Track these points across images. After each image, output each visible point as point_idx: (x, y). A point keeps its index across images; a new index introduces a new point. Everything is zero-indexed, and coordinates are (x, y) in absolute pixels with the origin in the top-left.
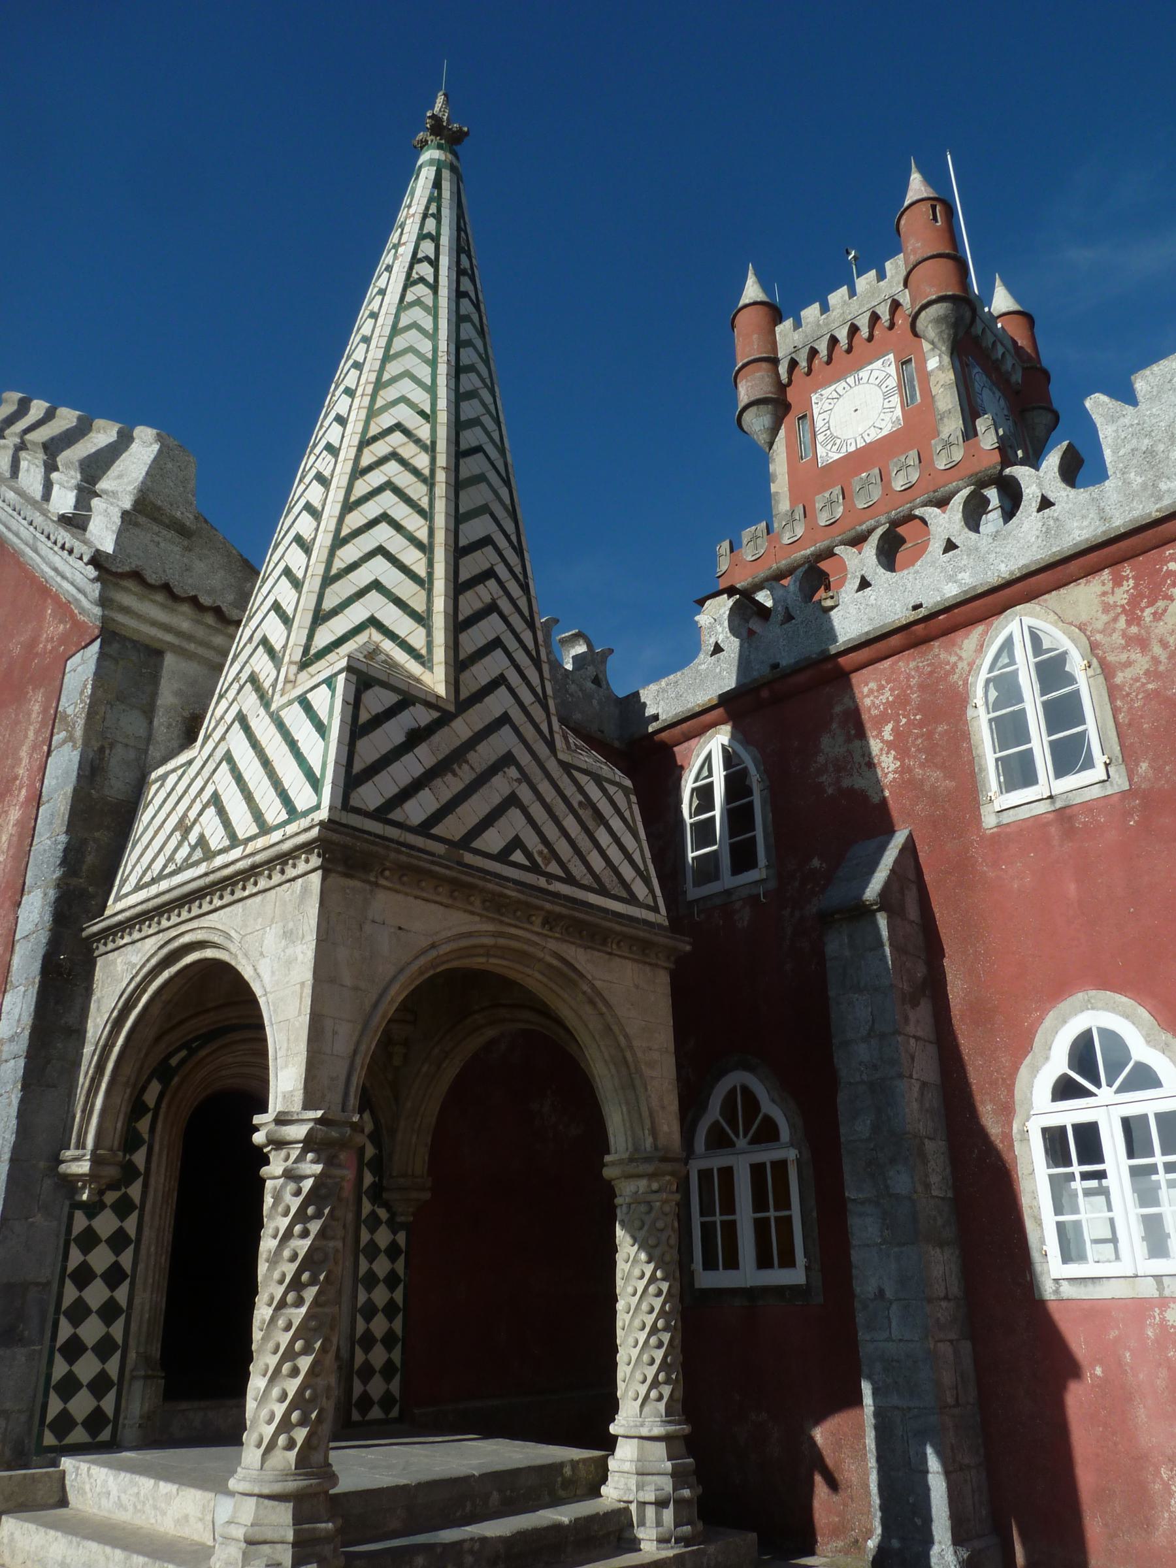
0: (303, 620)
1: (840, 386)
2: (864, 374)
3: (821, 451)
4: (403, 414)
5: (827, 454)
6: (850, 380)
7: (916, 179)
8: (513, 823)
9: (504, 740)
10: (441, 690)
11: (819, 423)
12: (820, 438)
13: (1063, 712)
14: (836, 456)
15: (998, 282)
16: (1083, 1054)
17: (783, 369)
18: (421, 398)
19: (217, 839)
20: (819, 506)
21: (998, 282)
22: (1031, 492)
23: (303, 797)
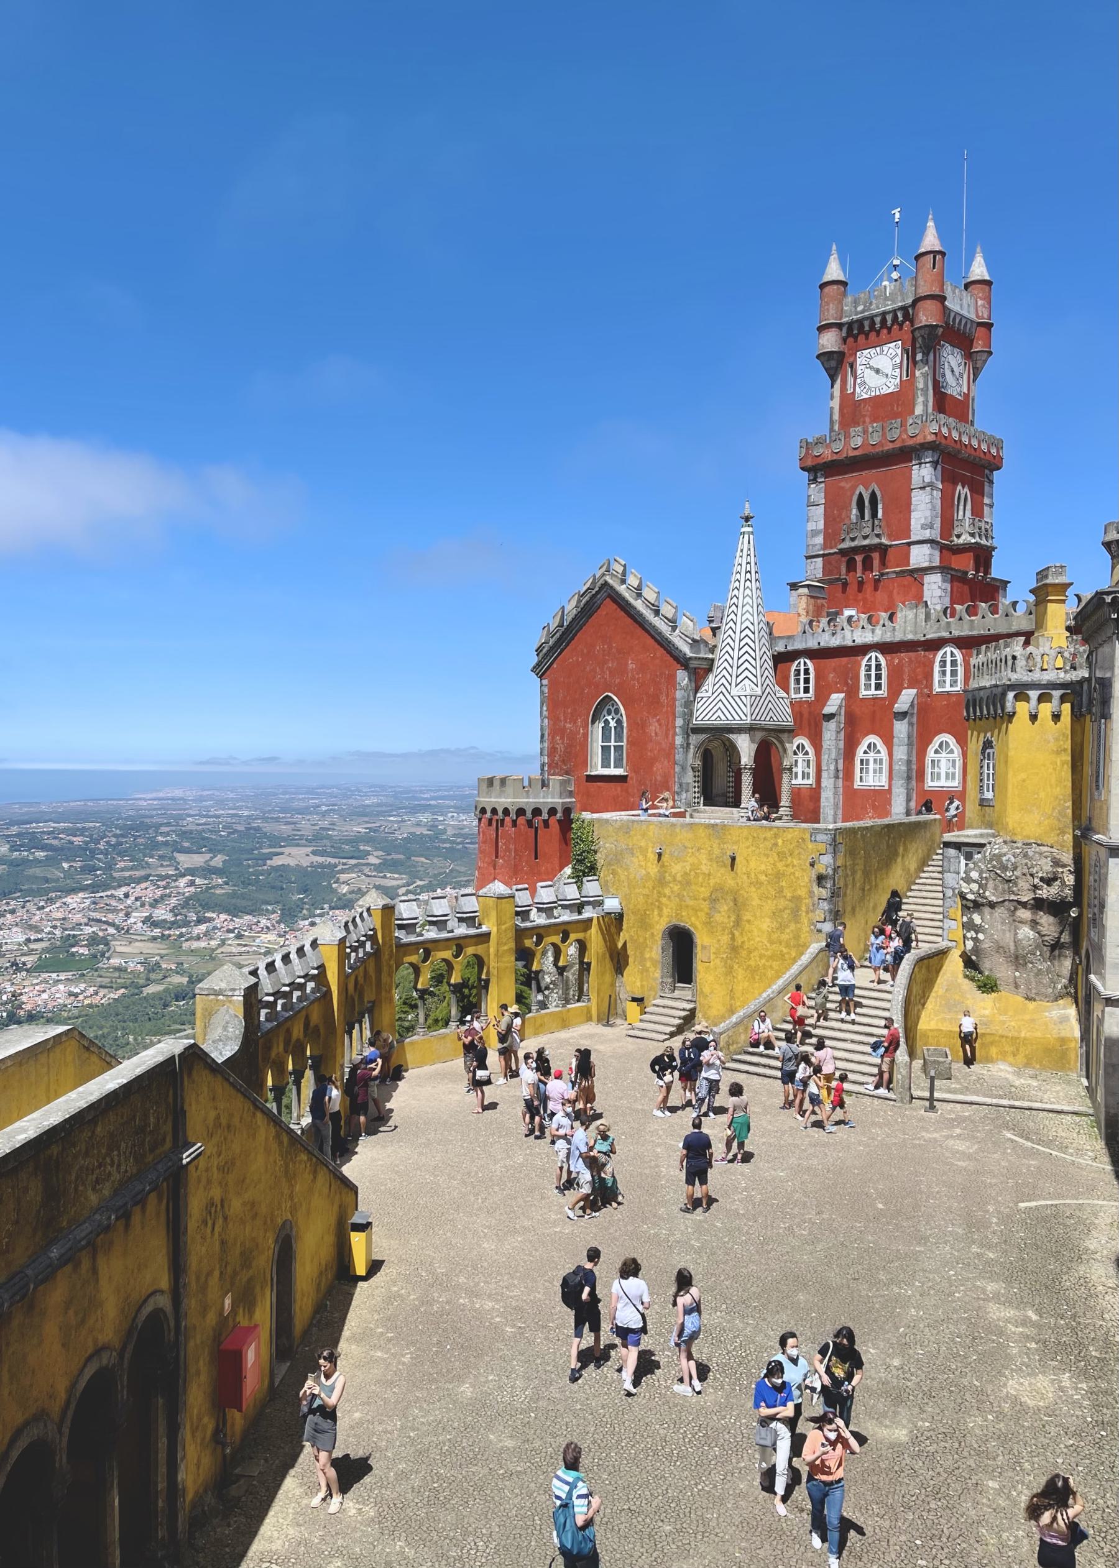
0: (734, 676)
1: (872, 351)
2: (885, 348)
3: (858, 390)
4: (747, 624)
5: (862, 394)
6: (878, 349)
7: (931, 224)
8: (771, 713)
9: (769, 697)
10: (760, 693)
11: (859, 372)
12: (858, 381)
13: (878, 677)
14: (865, 396)
15: (978, 249)
16: (869, 746)
17: (845, 329)
18: (751, 618)
19: (723, 718)
20: (852, 434)
21: (978, 249)
22: (881, 622)
23: (744, 717)
